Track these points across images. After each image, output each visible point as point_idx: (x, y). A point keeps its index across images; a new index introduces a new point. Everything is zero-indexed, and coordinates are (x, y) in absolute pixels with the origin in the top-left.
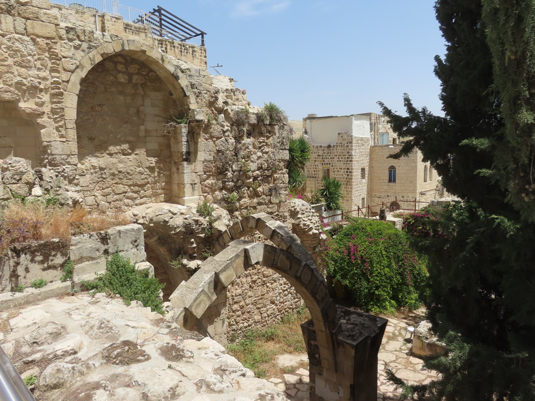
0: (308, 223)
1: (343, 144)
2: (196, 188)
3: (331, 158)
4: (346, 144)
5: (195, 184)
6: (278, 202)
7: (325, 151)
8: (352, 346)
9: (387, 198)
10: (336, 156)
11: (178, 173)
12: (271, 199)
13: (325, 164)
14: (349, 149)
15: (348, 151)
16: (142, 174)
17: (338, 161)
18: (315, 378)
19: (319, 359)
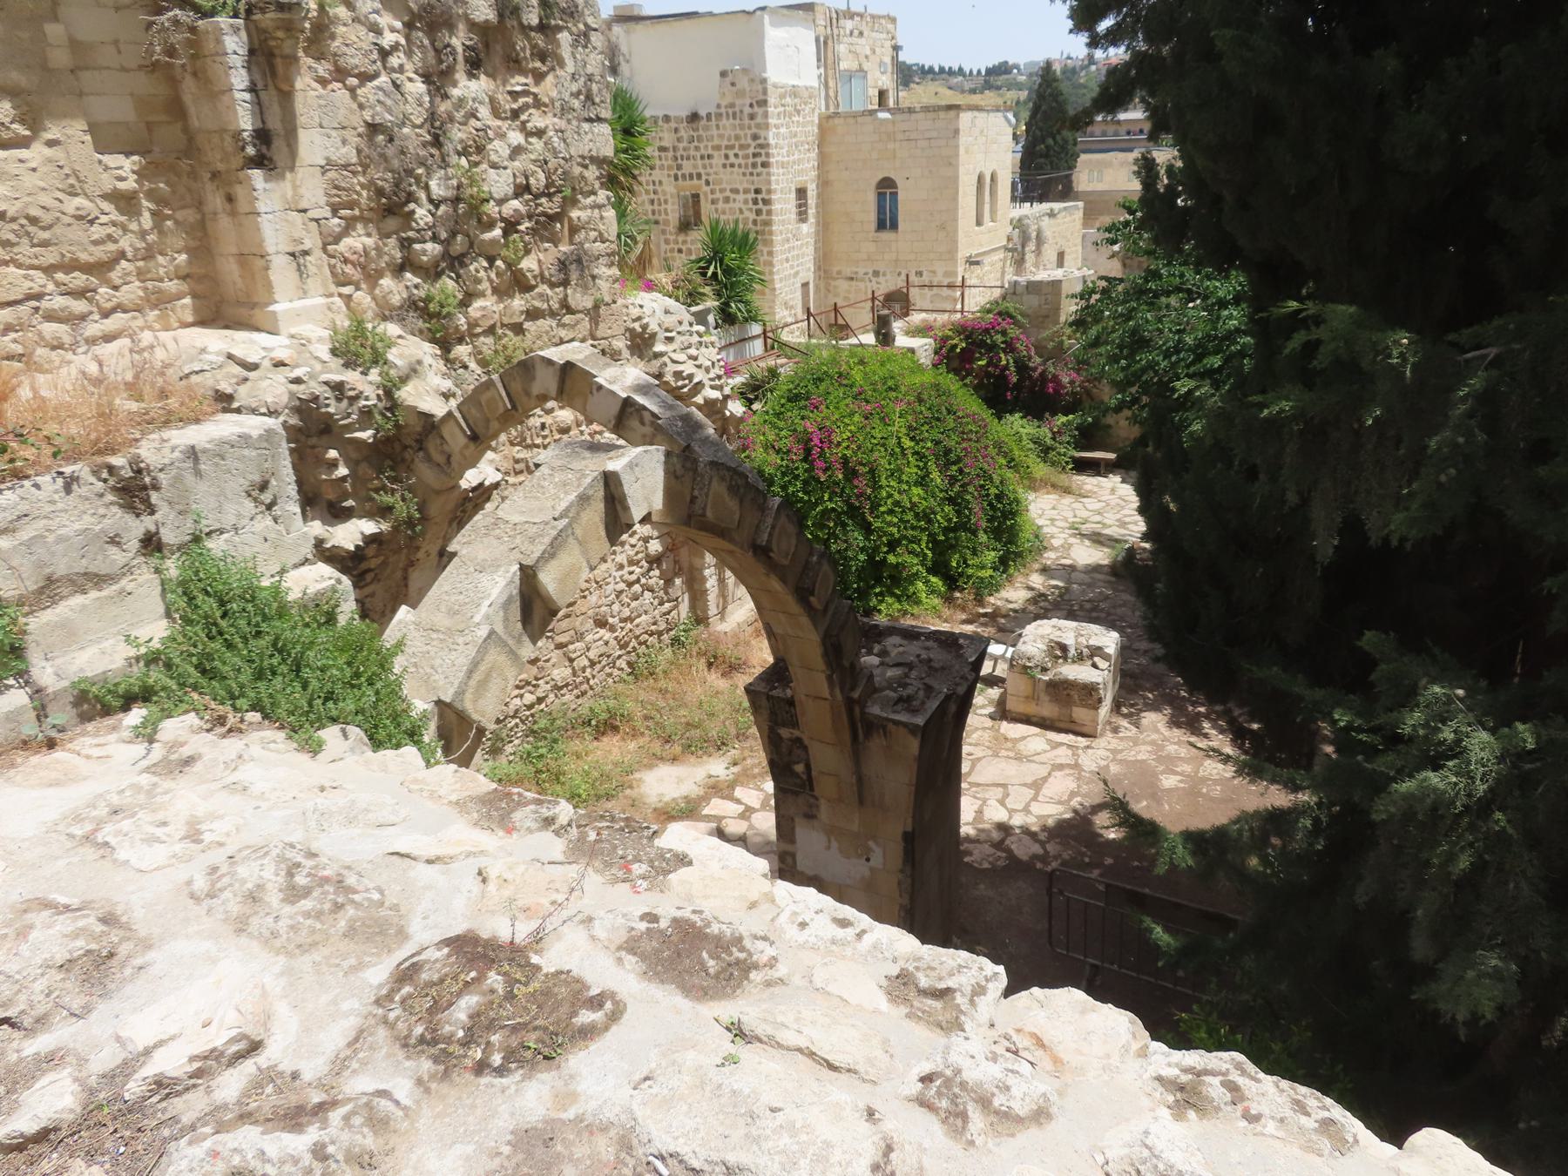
0: (688, 368)
1: (737, 109)
2: (312, 269)
3: (702, 157)
4: (747, 110)
5: (306, 253)
6: (589, 305)
7: (682, 133)
8: (913, 729)
9: (874, 279)
10: (718, 148)
11: (233, 214)
12: (566, 296)
13: (684, 176)
14: (758, 126)
15: (754, 130)
16: (91, 222)
17: (724, 166)
18: (793, 829)
19: (804, 777)
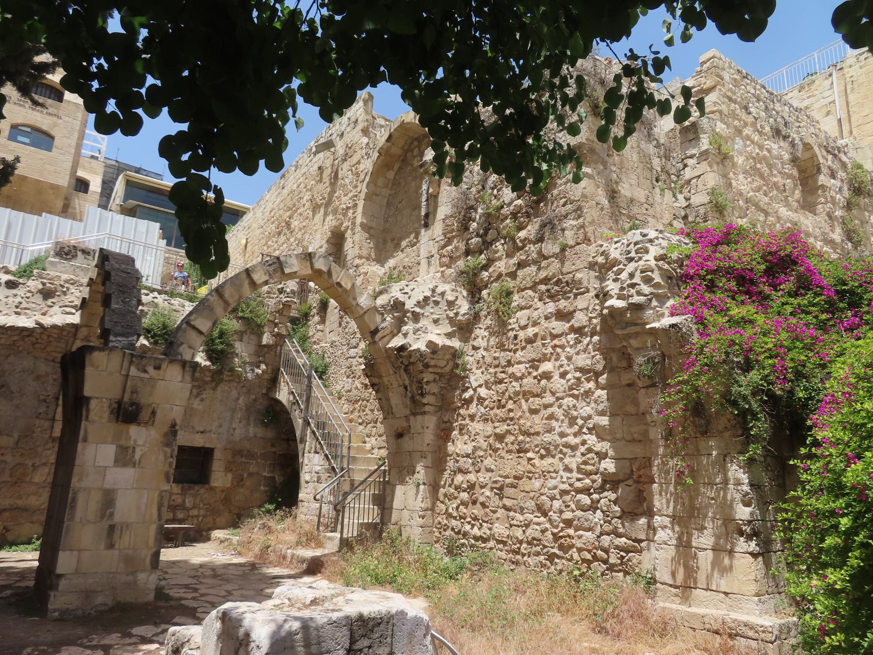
2: (433, 262)
5: (432, 256)
12: (541, 249)
